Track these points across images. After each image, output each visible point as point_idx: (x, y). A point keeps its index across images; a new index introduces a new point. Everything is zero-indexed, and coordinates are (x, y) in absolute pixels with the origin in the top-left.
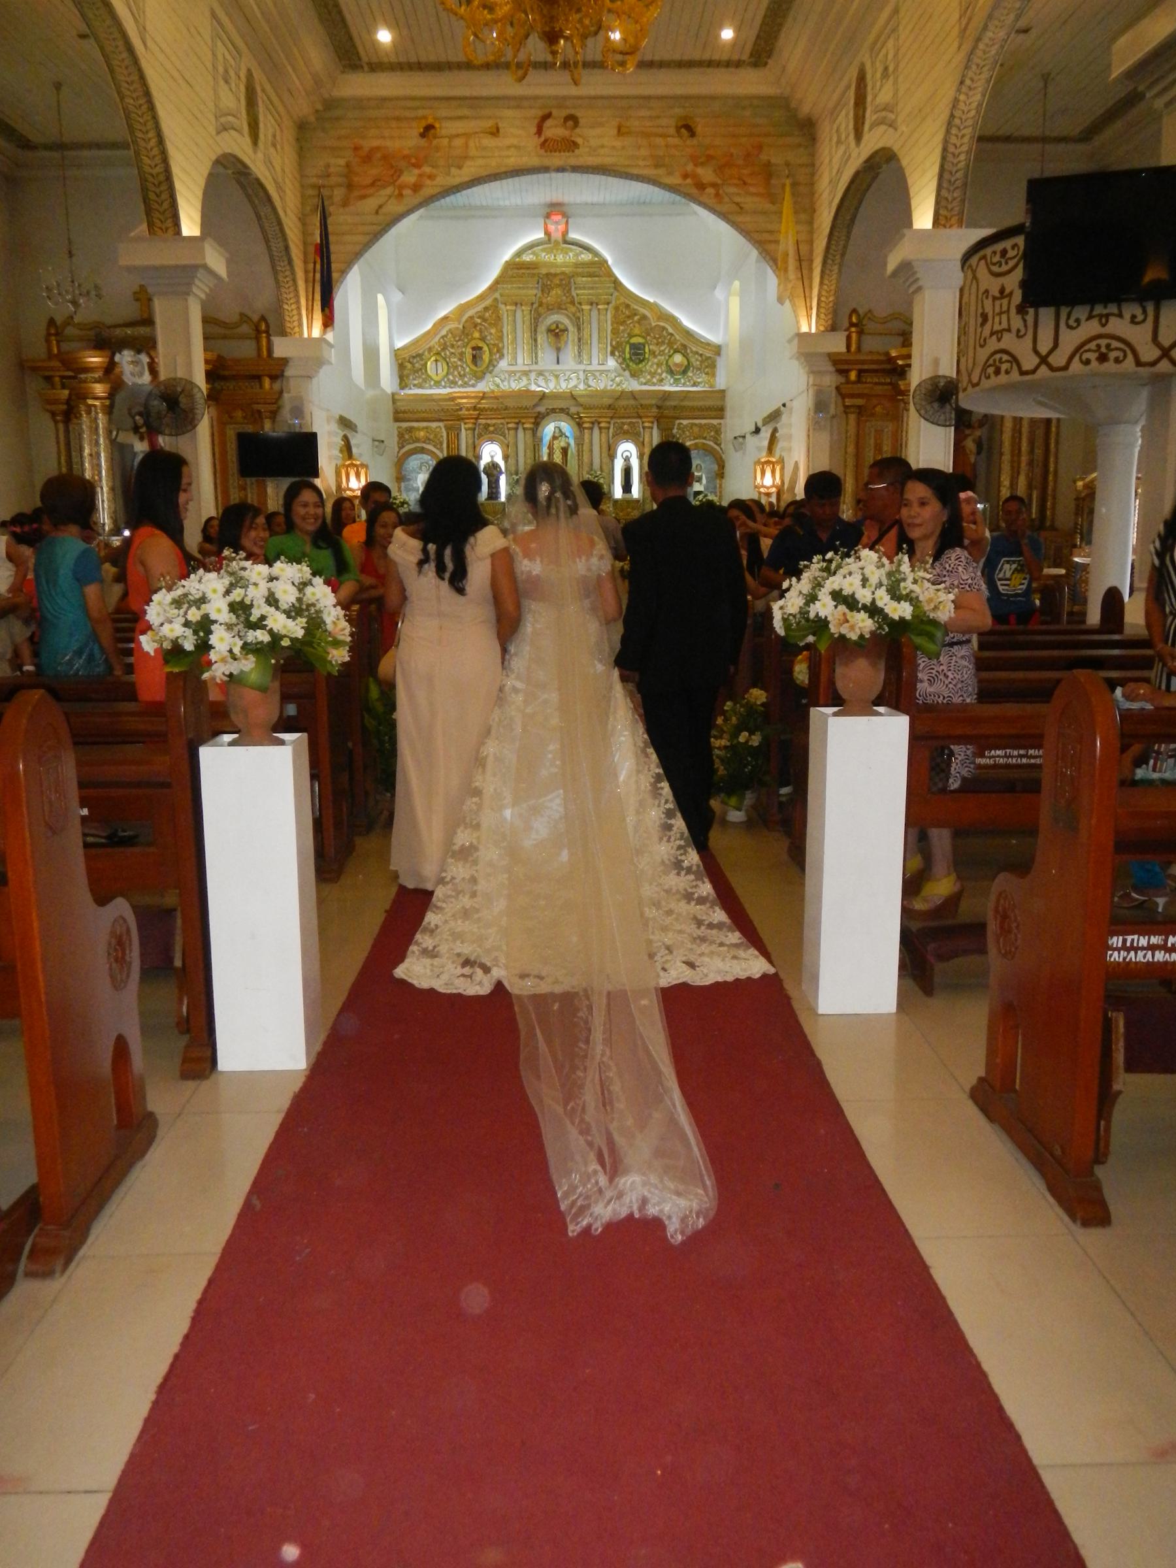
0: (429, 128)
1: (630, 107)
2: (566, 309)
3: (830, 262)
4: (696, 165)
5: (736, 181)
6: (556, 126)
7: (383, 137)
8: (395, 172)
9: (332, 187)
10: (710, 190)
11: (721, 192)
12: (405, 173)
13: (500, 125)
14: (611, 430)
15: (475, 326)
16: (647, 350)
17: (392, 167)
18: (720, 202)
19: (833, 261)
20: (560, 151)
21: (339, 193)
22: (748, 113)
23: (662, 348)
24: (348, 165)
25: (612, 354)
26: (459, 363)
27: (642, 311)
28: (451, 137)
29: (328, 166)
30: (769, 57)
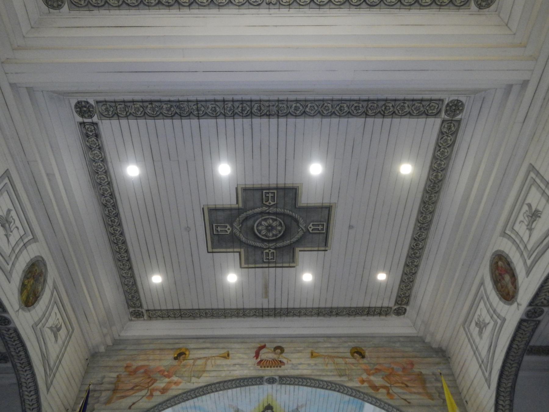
0: (180, 354)
1: (318, 342)
4: (369, 375)
5: (400, 385)
6: (268, 353)
7: (148, 360)
8: (152, 380)
9: (101, 391)
11: (391, 391)
12: (158, 382)
13: (230, 352)
18: (392, 399)
20: (271, 367)
21: (105, 395)
22: (398, 345)
24: (118, 377)
28: (195, 359)
30: (407, 303)
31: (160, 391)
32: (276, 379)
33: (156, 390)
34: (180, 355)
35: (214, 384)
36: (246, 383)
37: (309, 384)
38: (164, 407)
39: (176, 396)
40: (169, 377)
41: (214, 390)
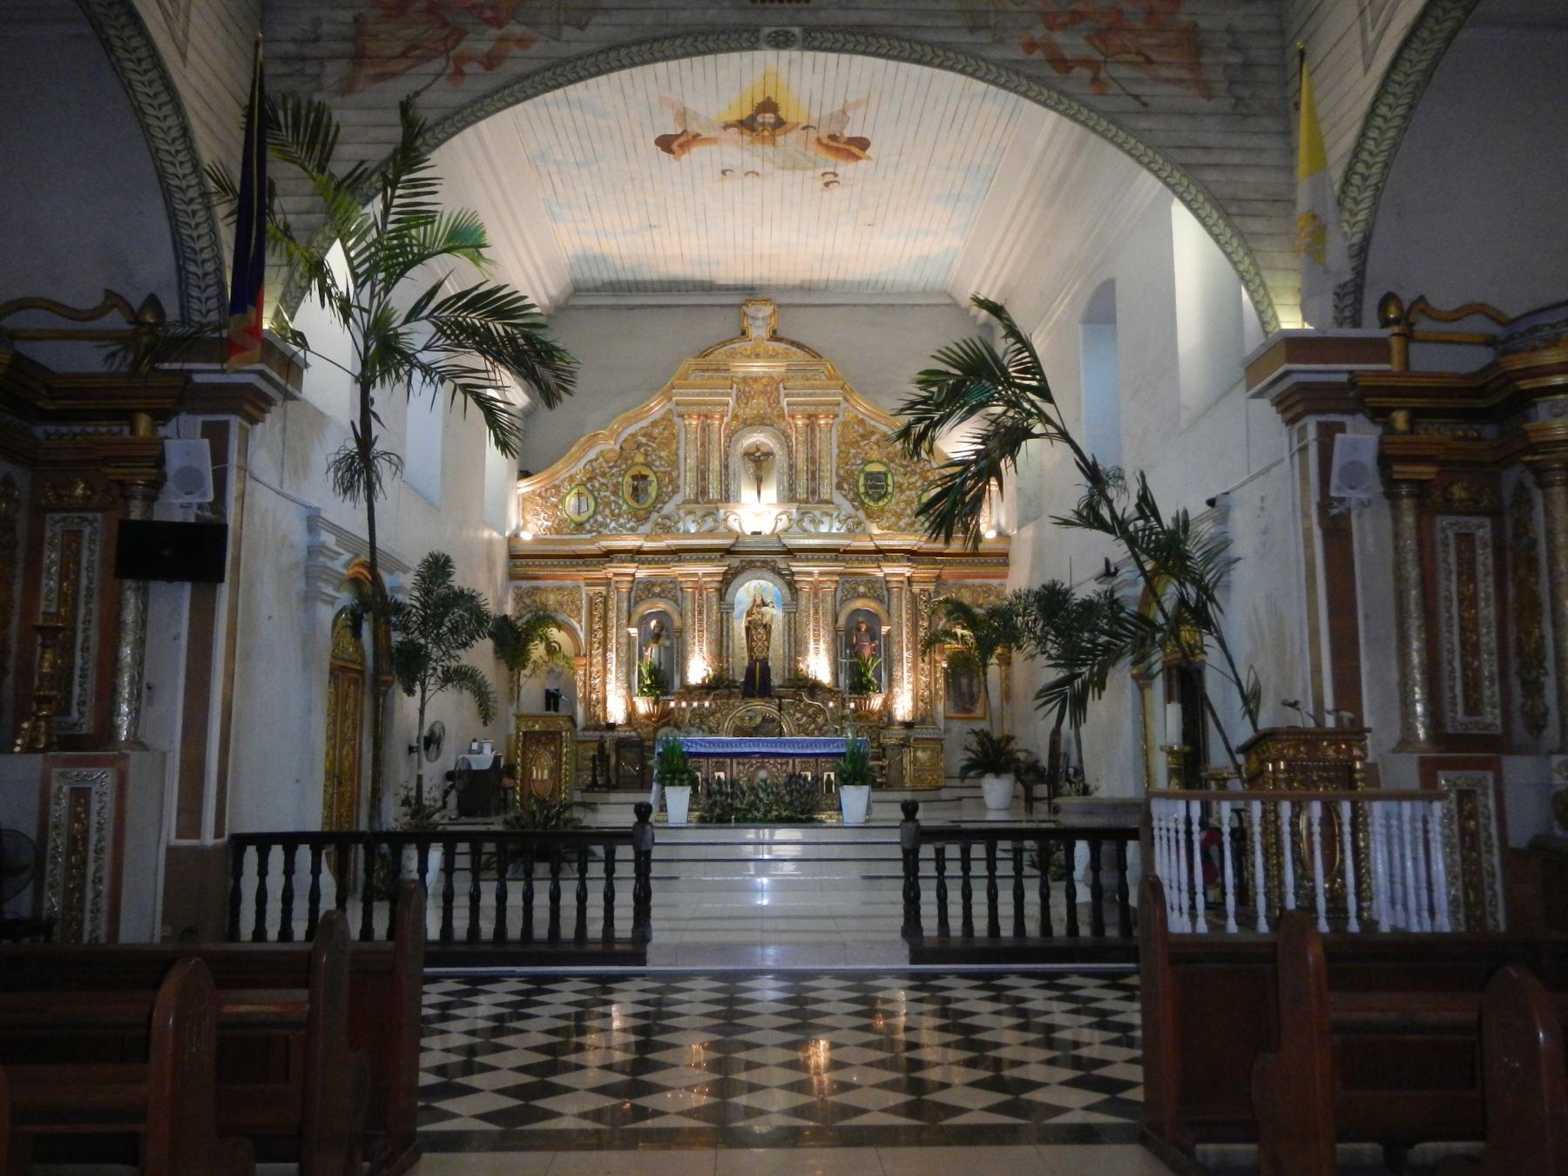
2: (772, 425)
3: (1356, 180)
4: (1051, 28)
10: (1076, 71)
11: (1102, 75)
14: (839, 594)
15: (639, 446)
16: (890, 481)
17: (445, 24)
18: (1102, 94)
19: (1364, 178)
21: (335, 71)
23: (913, 480)
24: (356, 20)
25: (839, 487)
26: (613, 498)
31: (480, 62)
32: (793, 35)
33: (471, 59)
35: (626, 45)
36: (711, 45)
37: (884, 51)
38: (499, 105)
39: (527, 76)
40: (498, 23)
41: (625, 62)
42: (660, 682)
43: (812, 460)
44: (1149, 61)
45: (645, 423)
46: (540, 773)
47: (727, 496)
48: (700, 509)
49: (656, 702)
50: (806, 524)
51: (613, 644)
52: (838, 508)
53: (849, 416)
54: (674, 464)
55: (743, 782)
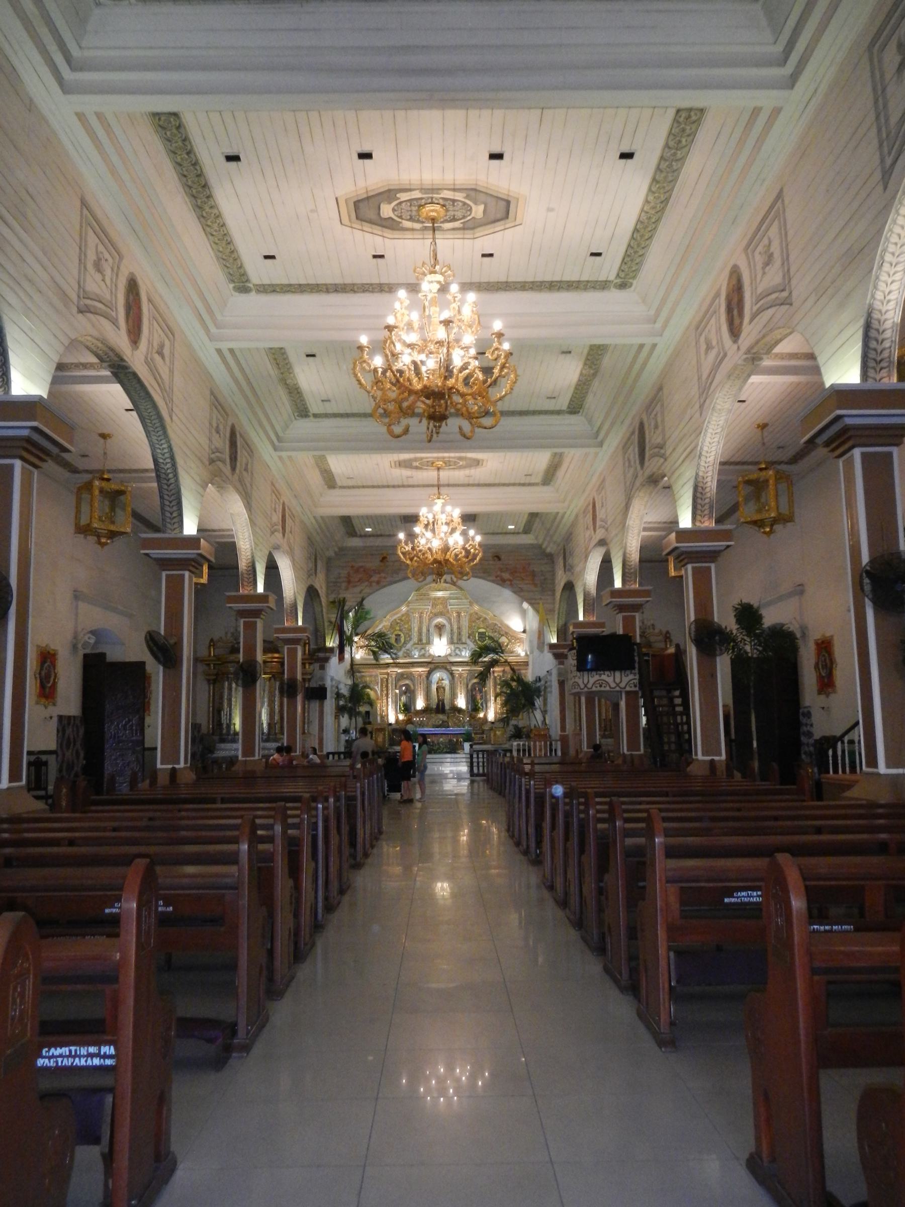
4: (501, 572)
15: (398, 623)
21: (344, 585)
24: (349, 574)
27: (484, 616)
29: (339, 574)
34: (384, 559)
40: (380, 574)
42: (407, 708)
43: (459, 628)
44: (523, 579)
45: (398, 615)
46: (380, 739)
47: (429, 642)
48: (419, 647)
49: (406, 716)
50: (458, 653)
51: (390, 696)
52: (468, 645)
53: (472, 611)
54: (410, 630)
55: (436, 742)
